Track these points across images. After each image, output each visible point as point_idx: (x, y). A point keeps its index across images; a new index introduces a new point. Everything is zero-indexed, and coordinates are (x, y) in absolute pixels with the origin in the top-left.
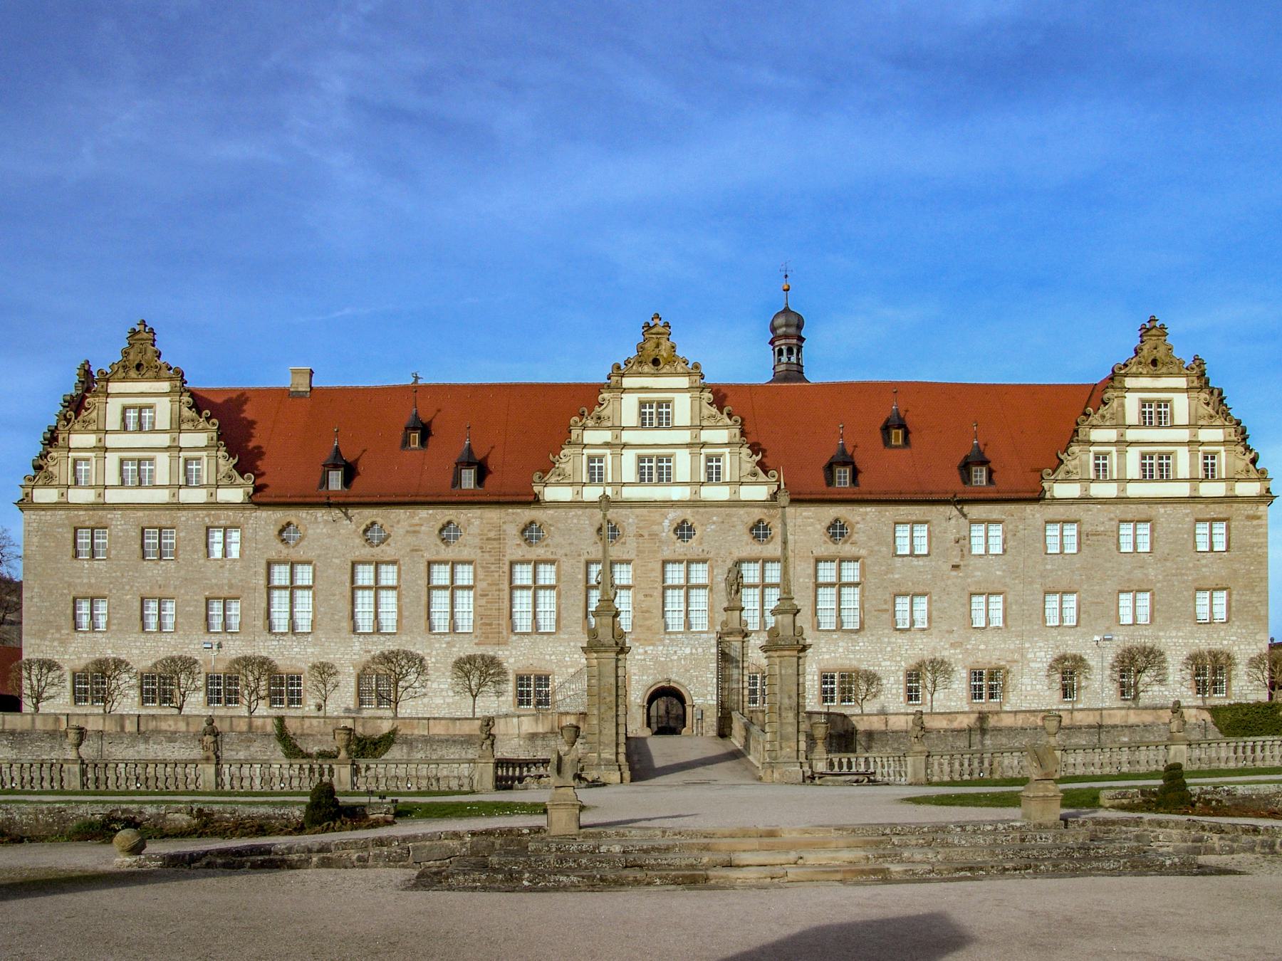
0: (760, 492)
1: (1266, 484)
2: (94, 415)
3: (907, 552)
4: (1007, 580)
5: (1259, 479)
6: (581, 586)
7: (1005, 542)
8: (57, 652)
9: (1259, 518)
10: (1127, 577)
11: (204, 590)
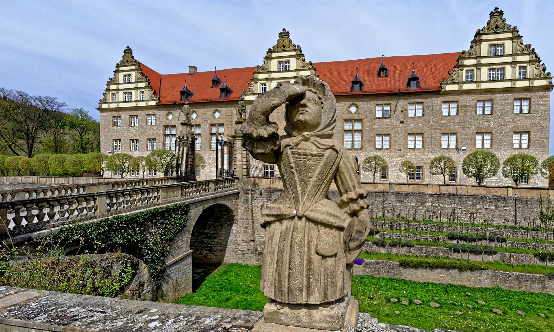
3: (381, 116)
4: (425, 128)
7: (423, 111)
9: (546, 97)
10: (480, 126)
11: (146, 135)
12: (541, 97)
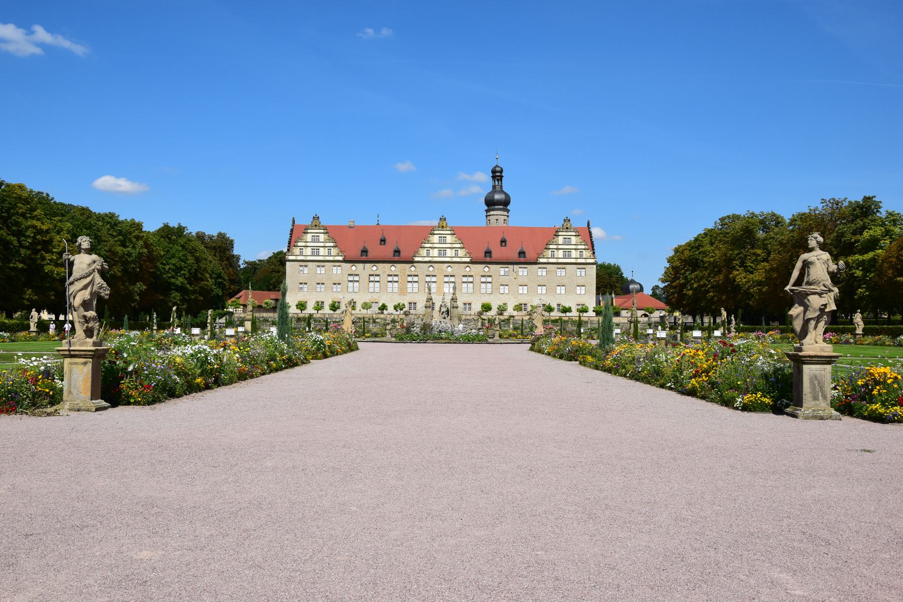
1: (596, 260)
2: (304, 238)
5: (593, 259)
6: (424, 281)
12: (591, 268)
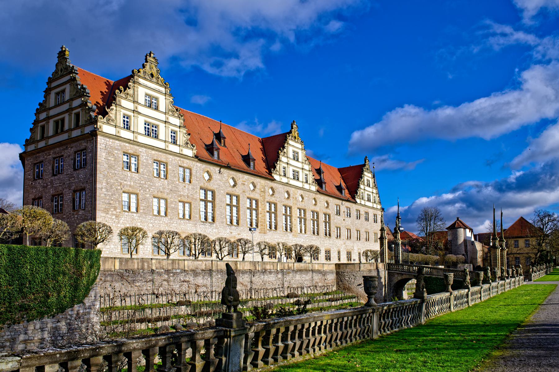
0: (314, 188)
8: (114, 222)
